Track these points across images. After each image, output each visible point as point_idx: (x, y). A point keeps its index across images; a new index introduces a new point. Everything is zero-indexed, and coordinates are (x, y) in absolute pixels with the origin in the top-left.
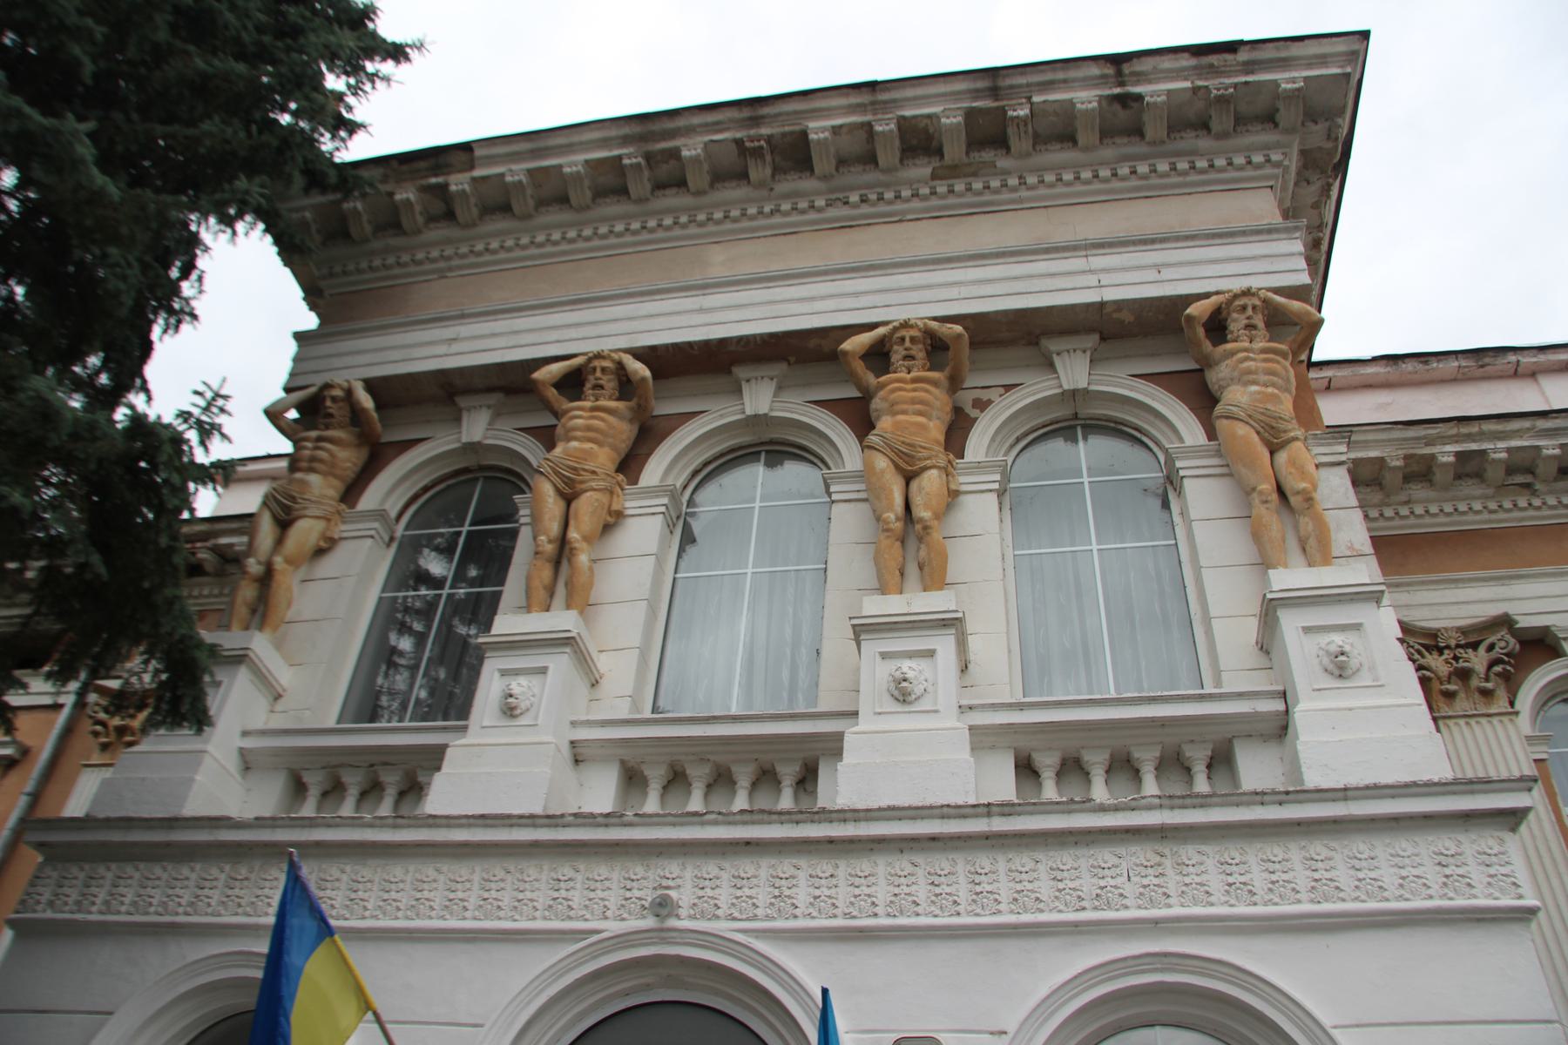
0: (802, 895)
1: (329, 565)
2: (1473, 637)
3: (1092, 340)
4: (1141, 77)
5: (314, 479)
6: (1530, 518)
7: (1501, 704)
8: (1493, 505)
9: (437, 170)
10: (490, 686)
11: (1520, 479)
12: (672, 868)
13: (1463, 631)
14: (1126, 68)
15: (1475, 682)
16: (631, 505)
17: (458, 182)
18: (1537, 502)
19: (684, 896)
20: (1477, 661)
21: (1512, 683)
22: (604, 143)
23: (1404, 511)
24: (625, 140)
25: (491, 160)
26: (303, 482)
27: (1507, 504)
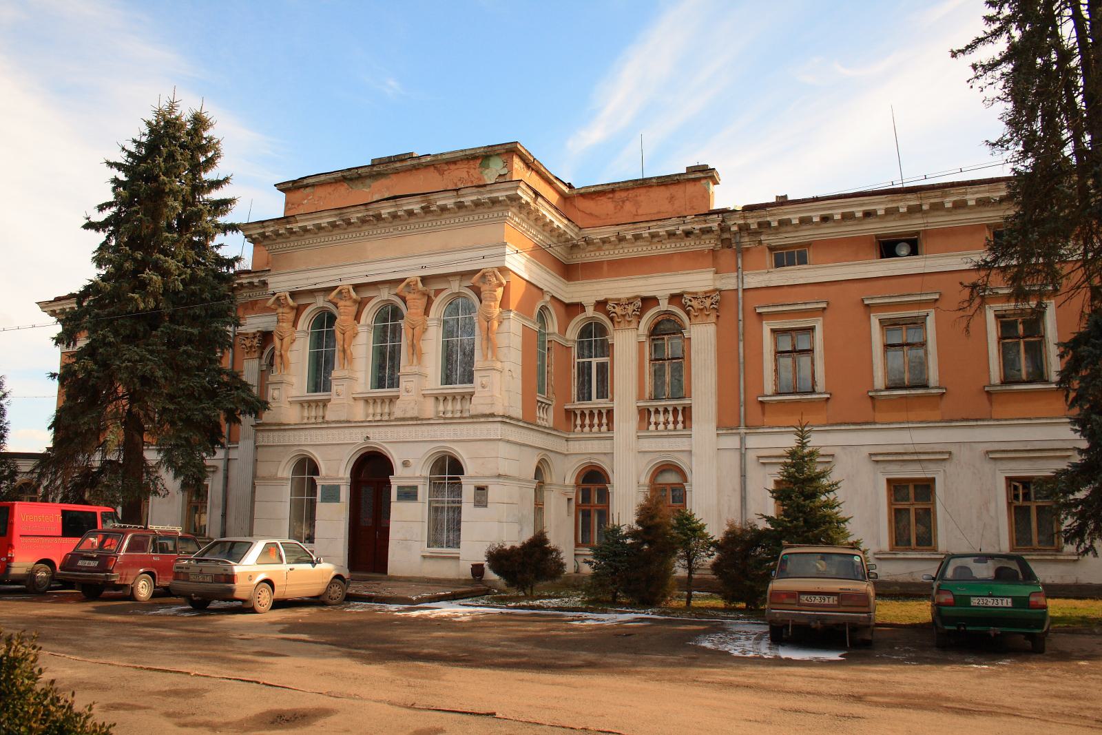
0: (389, 435)
1: (295, 346)
2: (630, 301)
3: (458, 278)
4: (463, 196)
5: (284, 325)
6: (662, 252)
7: (634, 325)
8: (649, 248)
9: (289, 223)
10: (334, 388)
11: (657, 239)
12: (369, 430)
13: (628, 299)
14: (460, 193)
15: (627, 318)
16: (360, 329)
17: (295, 227)
18: (664, 247)
19: (371, 436)
20: (630, 309)
21: (640, 317)
22: (330, 216)
23: (621, 251)
24: (336, 215)
25: (302, 221)
26: (282, 327)
27: (654, 248)
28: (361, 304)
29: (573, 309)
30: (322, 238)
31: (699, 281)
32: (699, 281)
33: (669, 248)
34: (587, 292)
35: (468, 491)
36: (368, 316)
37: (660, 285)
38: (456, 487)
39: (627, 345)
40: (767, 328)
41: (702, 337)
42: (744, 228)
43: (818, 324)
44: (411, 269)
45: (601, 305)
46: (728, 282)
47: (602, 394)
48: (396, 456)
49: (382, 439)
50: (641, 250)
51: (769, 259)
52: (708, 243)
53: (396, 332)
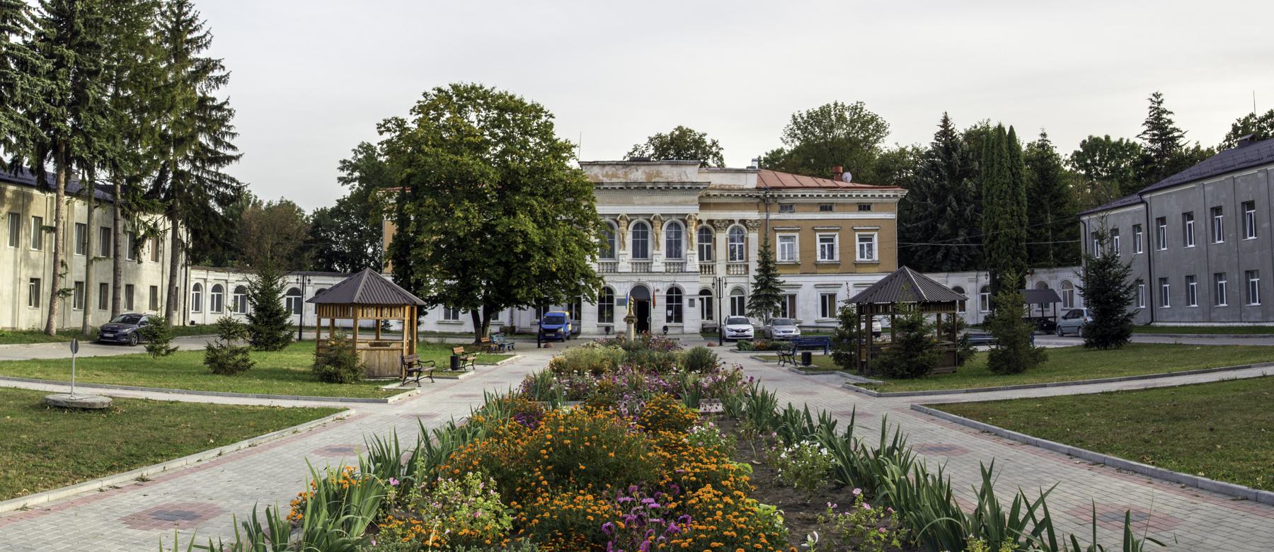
28: (629, 223)
29: (700, 222)
30: (612, 193)
31: (753, 215)
32: (753, 215)
33: (740, 201)
34: (705, 215)
35: (685, 302)
36: (631, 228)
37: (736, 215)
38: (679, 299)
39: (721, 238)
40: (778, 235)
41: (754, 237)
42: (772, 196)
43: (797, 235)
44: (657, 210)
45: (710, 222)
46: (764, 216)
47: (709, 258)
48: (652, 286)
49: (644, 279)
50: (729, 200)
51: (778, 207)
52: (758, 200)
53: (645, 235)
